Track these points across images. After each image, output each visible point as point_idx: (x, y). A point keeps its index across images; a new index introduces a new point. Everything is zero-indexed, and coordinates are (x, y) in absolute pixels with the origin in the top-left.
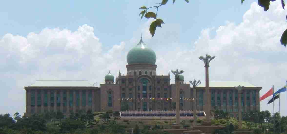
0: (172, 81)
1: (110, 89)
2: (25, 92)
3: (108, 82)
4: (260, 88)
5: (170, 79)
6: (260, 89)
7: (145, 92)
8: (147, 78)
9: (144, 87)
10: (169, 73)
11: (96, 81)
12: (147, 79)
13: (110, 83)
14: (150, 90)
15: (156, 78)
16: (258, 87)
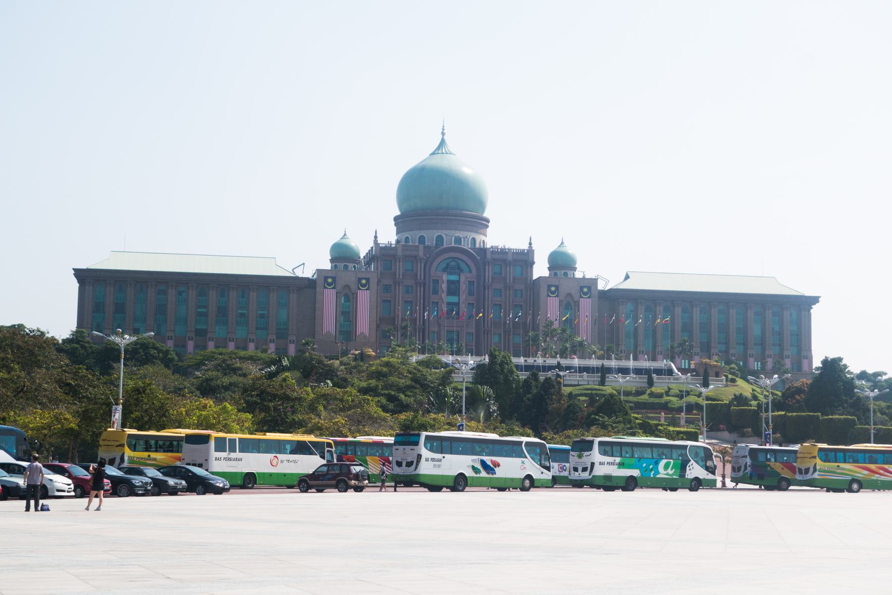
0: (541, 269)
1: (347, 286)
2: (75, 285)
3: (341, 265)
4: (815, 300)
5: (534, 263)
6: (815, 304)
7: (454, 299)
8: (465, 258)
9: (450, 282)
10: (530, 244)
11: (308, 259)
12: (462, 260)
13: (346, 267)
14: (470, 293)
15: (489, 256)
16: (807, 294)
